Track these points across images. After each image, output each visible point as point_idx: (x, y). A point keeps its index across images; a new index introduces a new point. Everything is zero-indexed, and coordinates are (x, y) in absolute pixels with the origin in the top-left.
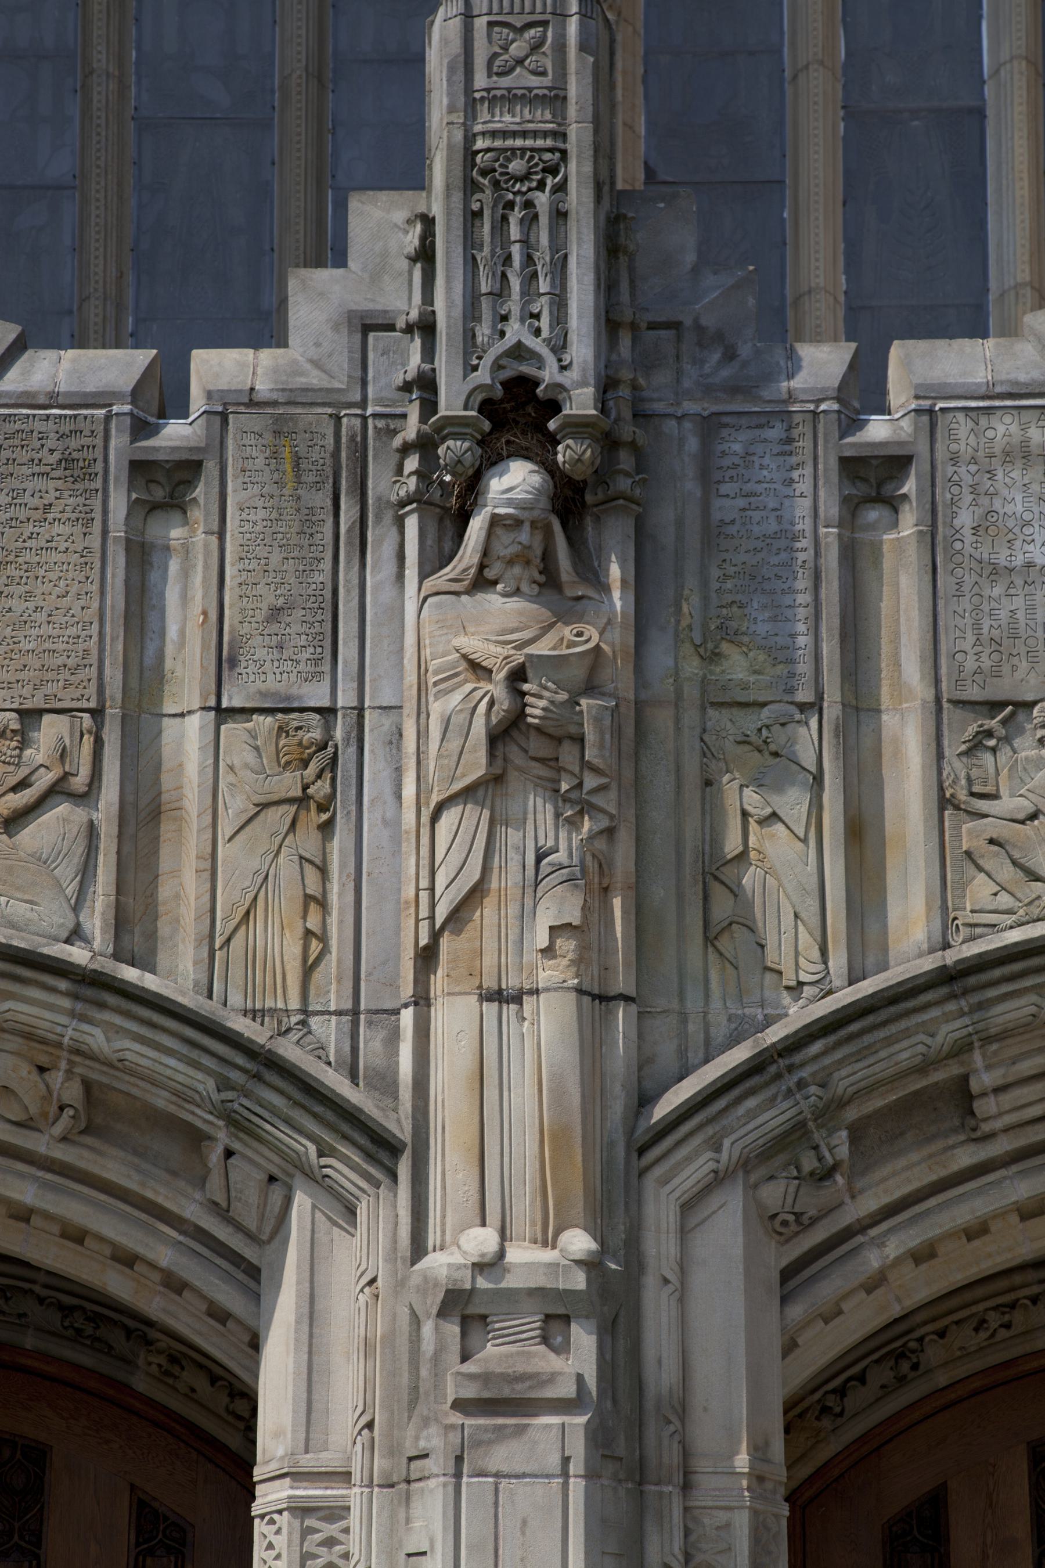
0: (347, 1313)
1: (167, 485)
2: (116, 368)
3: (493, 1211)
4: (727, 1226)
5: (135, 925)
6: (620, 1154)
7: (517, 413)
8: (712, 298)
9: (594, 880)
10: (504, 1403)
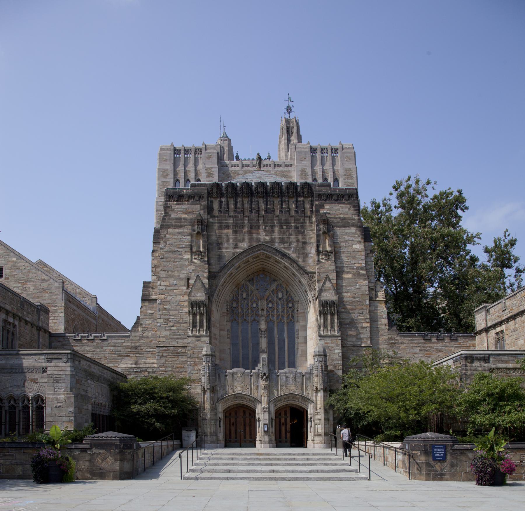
0: (259, 408)
1: (251, 376)
2: (249, 371)
3: (264, 405)
4: (273, 405)
5: (251, 394)
6: (269, 402)
7: (265, 374)
8: (272, 368)
9: (268, 392)
10: (265, 411)
